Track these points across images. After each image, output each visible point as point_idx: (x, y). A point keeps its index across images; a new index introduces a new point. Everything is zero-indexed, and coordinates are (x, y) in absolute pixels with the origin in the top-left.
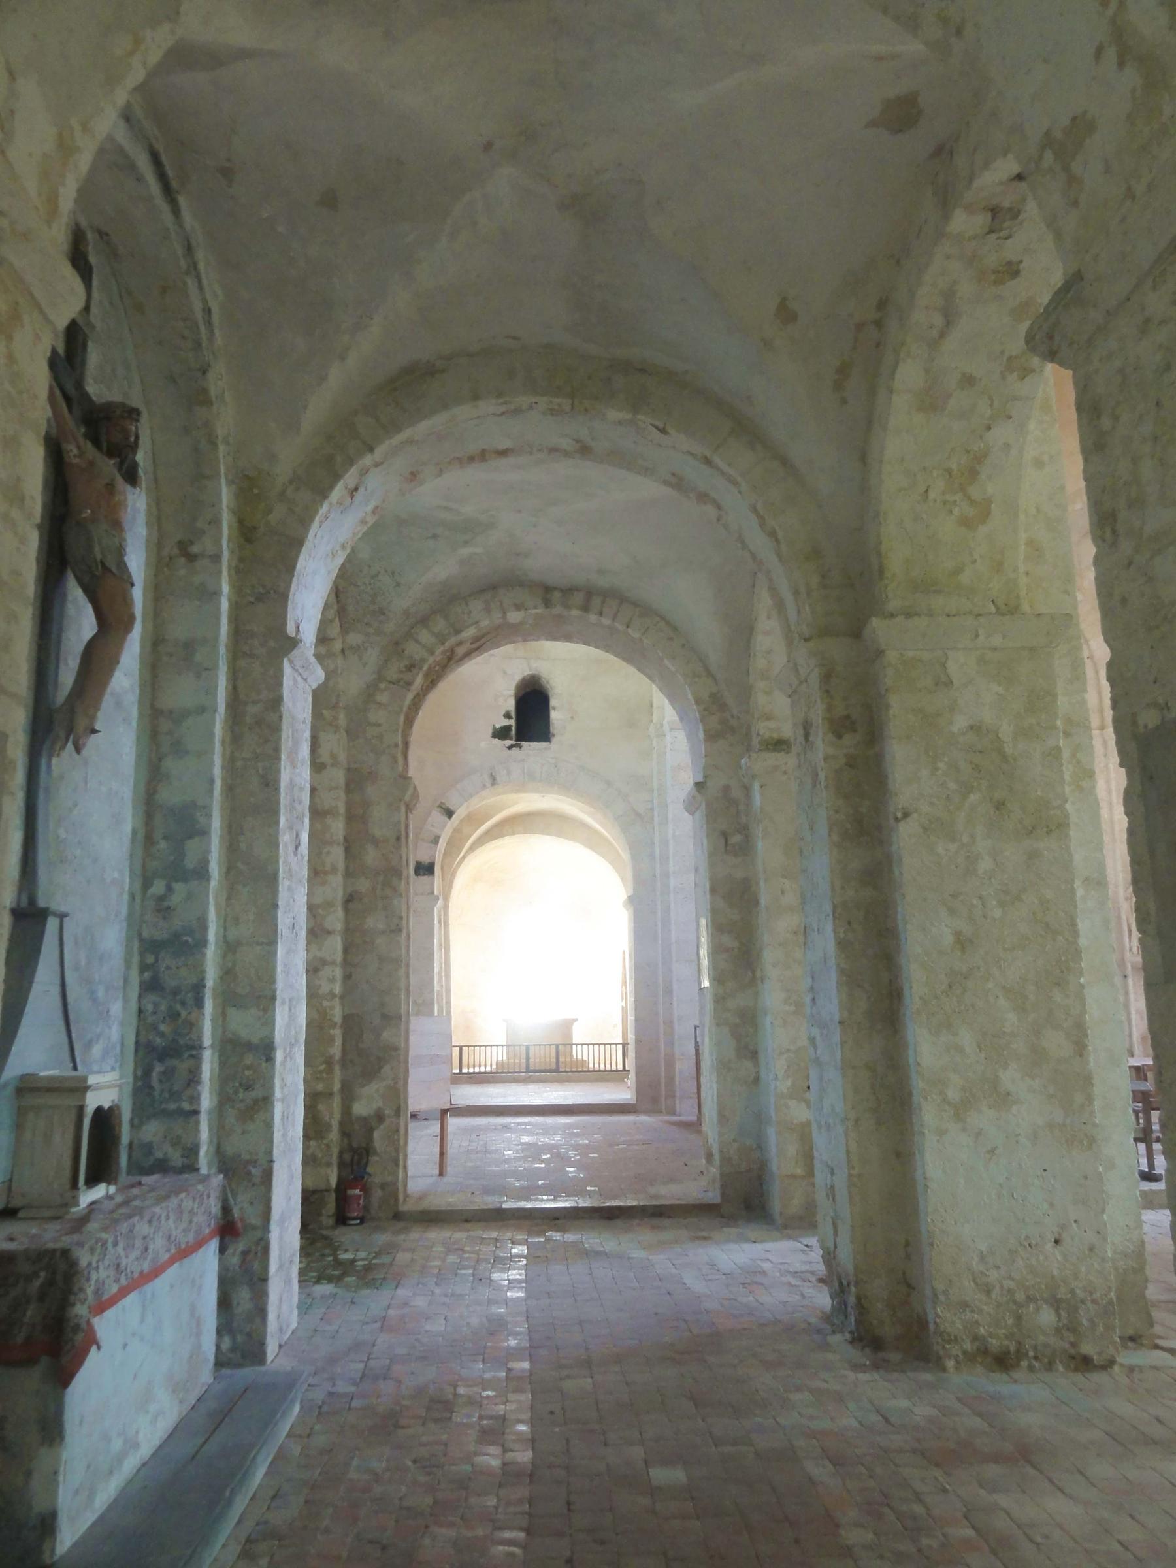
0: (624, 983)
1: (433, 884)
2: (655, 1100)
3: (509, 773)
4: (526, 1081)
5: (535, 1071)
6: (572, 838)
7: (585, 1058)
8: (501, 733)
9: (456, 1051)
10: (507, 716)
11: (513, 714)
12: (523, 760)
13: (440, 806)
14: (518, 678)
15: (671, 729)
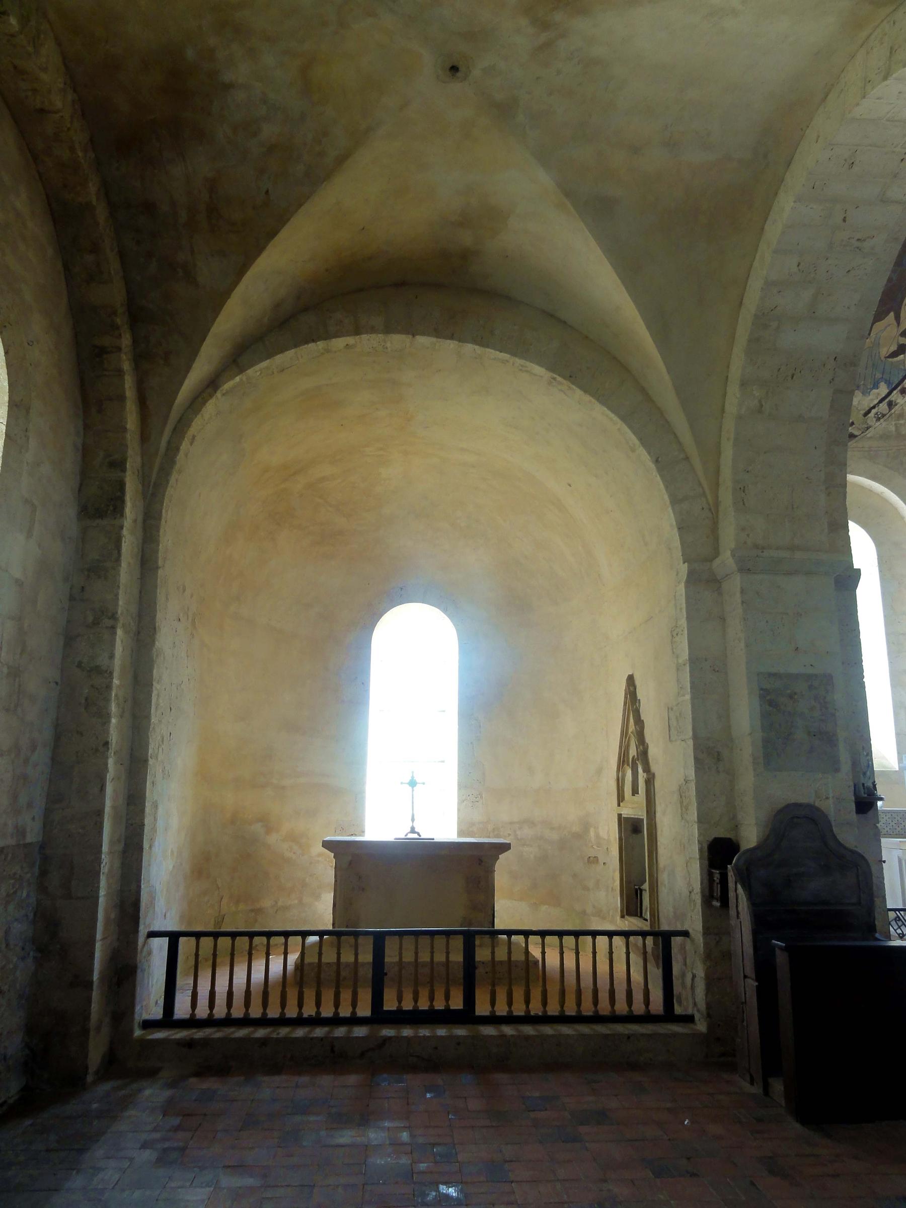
6: (519, 347)
9: (160, 946)
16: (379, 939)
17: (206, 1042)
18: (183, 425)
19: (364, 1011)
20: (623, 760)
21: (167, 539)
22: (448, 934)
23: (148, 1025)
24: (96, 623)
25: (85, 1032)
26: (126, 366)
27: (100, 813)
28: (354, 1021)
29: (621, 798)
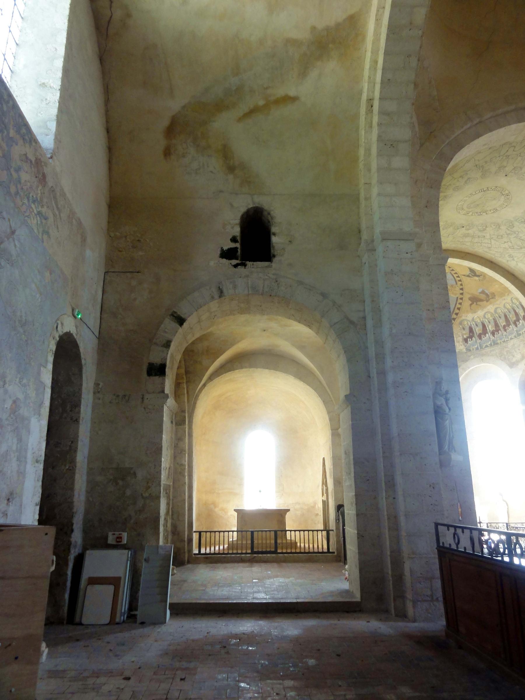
0: (325, 483)
1: (163, 384)
2: (381, 598)
3: (235, 287)
4: (252, 561)
5: (258, 553)
6: (286, 371)
7: (298, 540)
8: (227, 254)
9: (195, 536)
10: (234, 240)
11: (239, 239)
12: (247, 276)
13: (172, 315)
14: (243, 210)
15: (384, 240)
16: (252, 532)
17: (211, 557)
18: (197, 396)
19: (249, 551)
20: (323, 484)
21: (194, 427)
22: (270, 531)
23: (195, 554)
24: (181, 452)
25: (185, 552)
26: (185, 386)
27: (185, 500)
28: (246, 553)
29: (323, 495)
